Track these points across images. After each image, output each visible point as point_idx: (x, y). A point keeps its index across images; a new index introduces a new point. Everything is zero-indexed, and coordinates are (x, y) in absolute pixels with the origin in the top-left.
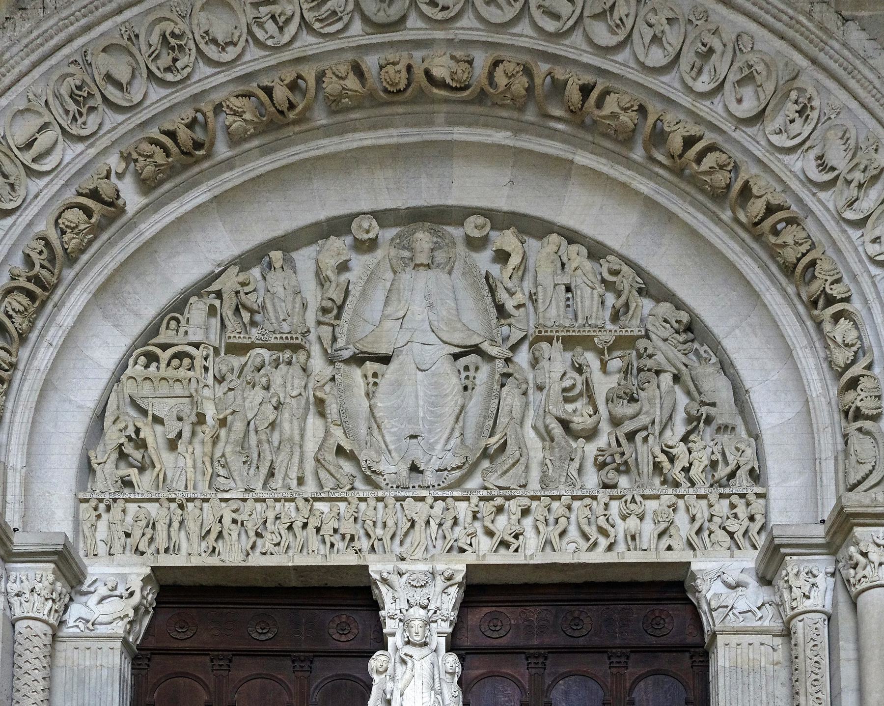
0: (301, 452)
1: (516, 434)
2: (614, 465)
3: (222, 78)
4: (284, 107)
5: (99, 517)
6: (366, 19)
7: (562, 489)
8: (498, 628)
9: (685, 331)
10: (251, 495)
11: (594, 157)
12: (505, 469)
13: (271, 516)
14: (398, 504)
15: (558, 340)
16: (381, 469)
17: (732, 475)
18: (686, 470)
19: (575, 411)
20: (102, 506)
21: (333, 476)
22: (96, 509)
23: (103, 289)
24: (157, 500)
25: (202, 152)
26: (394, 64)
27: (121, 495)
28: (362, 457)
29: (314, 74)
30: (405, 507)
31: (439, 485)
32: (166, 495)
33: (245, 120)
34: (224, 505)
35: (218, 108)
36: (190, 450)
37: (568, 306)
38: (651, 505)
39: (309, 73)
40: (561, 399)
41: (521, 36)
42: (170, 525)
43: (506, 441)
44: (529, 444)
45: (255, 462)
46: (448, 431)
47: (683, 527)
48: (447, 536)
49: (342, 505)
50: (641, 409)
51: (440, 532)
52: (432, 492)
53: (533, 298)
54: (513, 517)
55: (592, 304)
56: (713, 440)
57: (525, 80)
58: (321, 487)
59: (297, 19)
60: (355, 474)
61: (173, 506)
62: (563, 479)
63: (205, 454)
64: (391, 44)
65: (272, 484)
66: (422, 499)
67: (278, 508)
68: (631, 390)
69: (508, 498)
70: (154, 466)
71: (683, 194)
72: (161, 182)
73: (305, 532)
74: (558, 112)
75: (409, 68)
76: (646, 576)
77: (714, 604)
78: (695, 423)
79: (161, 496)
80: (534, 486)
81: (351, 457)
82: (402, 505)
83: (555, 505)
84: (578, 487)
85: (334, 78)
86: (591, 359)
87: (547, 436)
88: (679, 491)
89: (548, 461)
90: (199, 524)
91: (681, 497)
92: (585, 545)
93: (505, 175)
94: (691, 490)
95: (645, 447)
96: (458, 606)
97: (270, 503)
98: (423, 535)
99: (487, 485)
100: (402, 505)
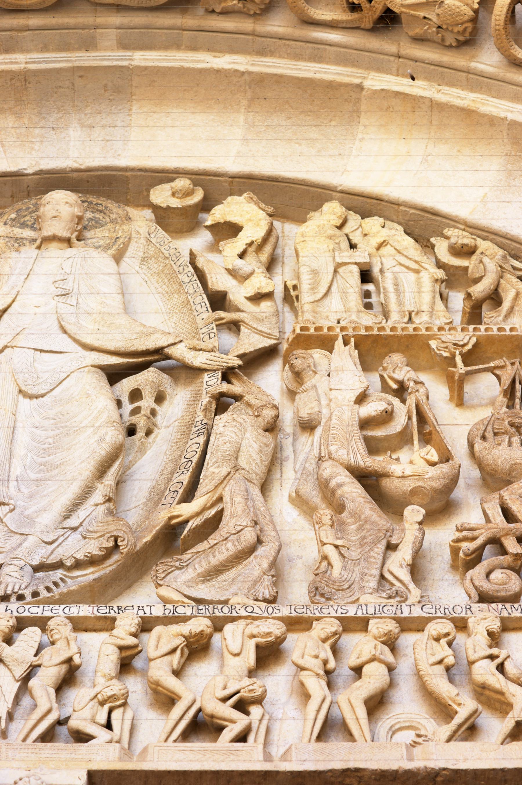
2: (507, 559)
31: (35, 594)
62: (372, 583)
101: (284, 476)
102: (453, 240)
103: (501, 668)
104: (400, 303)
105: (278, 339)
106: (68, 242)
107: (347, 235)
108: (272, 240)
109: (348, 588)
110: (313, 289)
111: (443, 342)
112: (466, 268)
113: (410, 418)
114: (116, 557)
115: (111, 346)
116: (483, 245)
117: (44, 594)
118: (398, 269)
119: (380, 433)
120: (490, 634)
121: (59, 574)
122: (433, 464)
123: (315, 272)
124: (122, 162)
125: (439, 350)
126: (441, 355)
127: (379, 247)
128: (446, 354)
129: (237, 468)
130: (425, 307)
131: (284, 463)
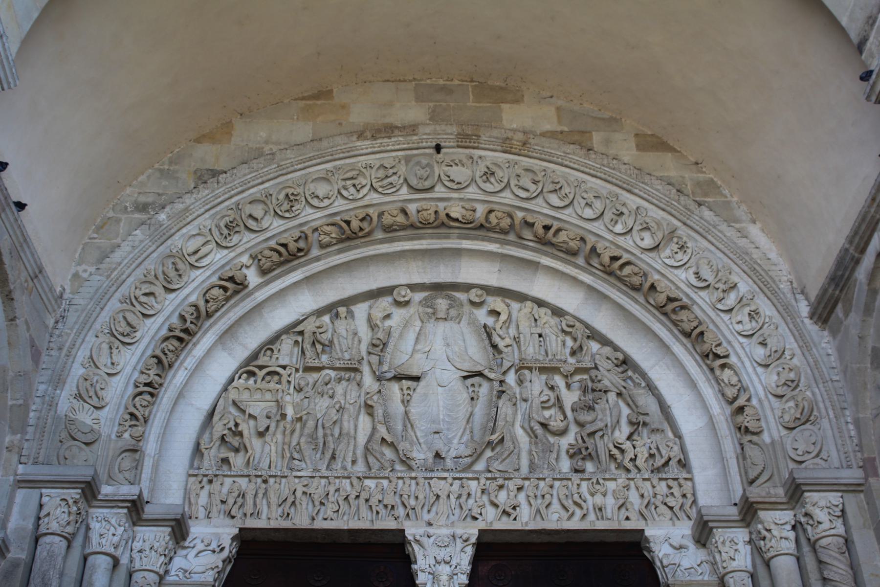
0: (355, 443)
1: (510, 433)
2: (581, 456)
3: (319, 214)
4: (357, 230)
5: (202, 488)
6: (410, 186)
7: (546, 473)
8: (502, 578)
9: (621, 365)
10: (317, 474)
11: (554, 261)
12: (503, 457)
13: (332, 489)
14: (427, 481)
15: (536, 369)
16: (414, 456)
17: (666, 464)
18: (633, 460)
19: (550, 417)
20: (205, 479)
21: (379, 461)
22: (200, 482)
23: (226, 332)
24: (248, 476)
25: (302, 254)
26: (426, 210)
27: (220, 472)
28: (400, 447)
29: (376, 214)
30: (432, 485)
32: (255, 473)
33: (331, 238)
34: (297, 480)
35: (316, 230)
36: (275, 440)
37: (541, 346)
38: (611, 485)
39: (373, 213)
40: (540, 409)
41: (505, 198)
42: (256, 495)
43: (503, 438)
44: (519, 438)
45: (321, 449)
46: (462, 430)
47: (633, 497)
48: (464, 507)
49: (385, 482)
50: (597, 417)
51: (458, 503)
52: (451, 474)
53: (517, 340)
54: (511, 493)
55: (557, 346)
56: (649, 438)
57: (509, 221)
58: (370, 468)
59: (369, 184)
60: (394, 459)
61: (259, 480)
62: (546, 466)
63: (284, 444)
64: (425, 199)
65: (334, 466)
66: (445, 478)
67: (337, 484)
68: (589, 404)
69: (505, 479)
70: (247, 451)
71: (613, 286)
72: (274, 269)
73: (357, 502)
74: (531, 238)
75: (436, 212)
76: (612, 538)
77: (665, 562)
78: (636, 427)
79: (251, 473)
80: (525, 470)
81: (392, 445)
82: (429, 483)
83: (542, 484)
84: (557, 472)
85: (390, 217)
86: (559, 381)
87: (532, 434)
88: (630, 476)
89: (534, 453)
90: (277, 495)
91: (633, 479)
92: (565, 515)
93: (496, 267)
94: (638, 475)
95: (602, 442)
96: (471, 561)
97: (332, 480)
98: (446, 507)
99: (491, 469)
100: (429, 483)
103: (580, 496)
104: (551, 350)
106: (445, 319)
110: (525, 344)
114: (475, 454)
115: (465, 369)
116: (578, 324)
117: (459, 469)
118: (550, 334)
120: (578, 485)
121: (461, 459)
122: (562, 421)
123: (525, 337)
124: (459, 281)
127: (545, 324)
129: (507, 422)
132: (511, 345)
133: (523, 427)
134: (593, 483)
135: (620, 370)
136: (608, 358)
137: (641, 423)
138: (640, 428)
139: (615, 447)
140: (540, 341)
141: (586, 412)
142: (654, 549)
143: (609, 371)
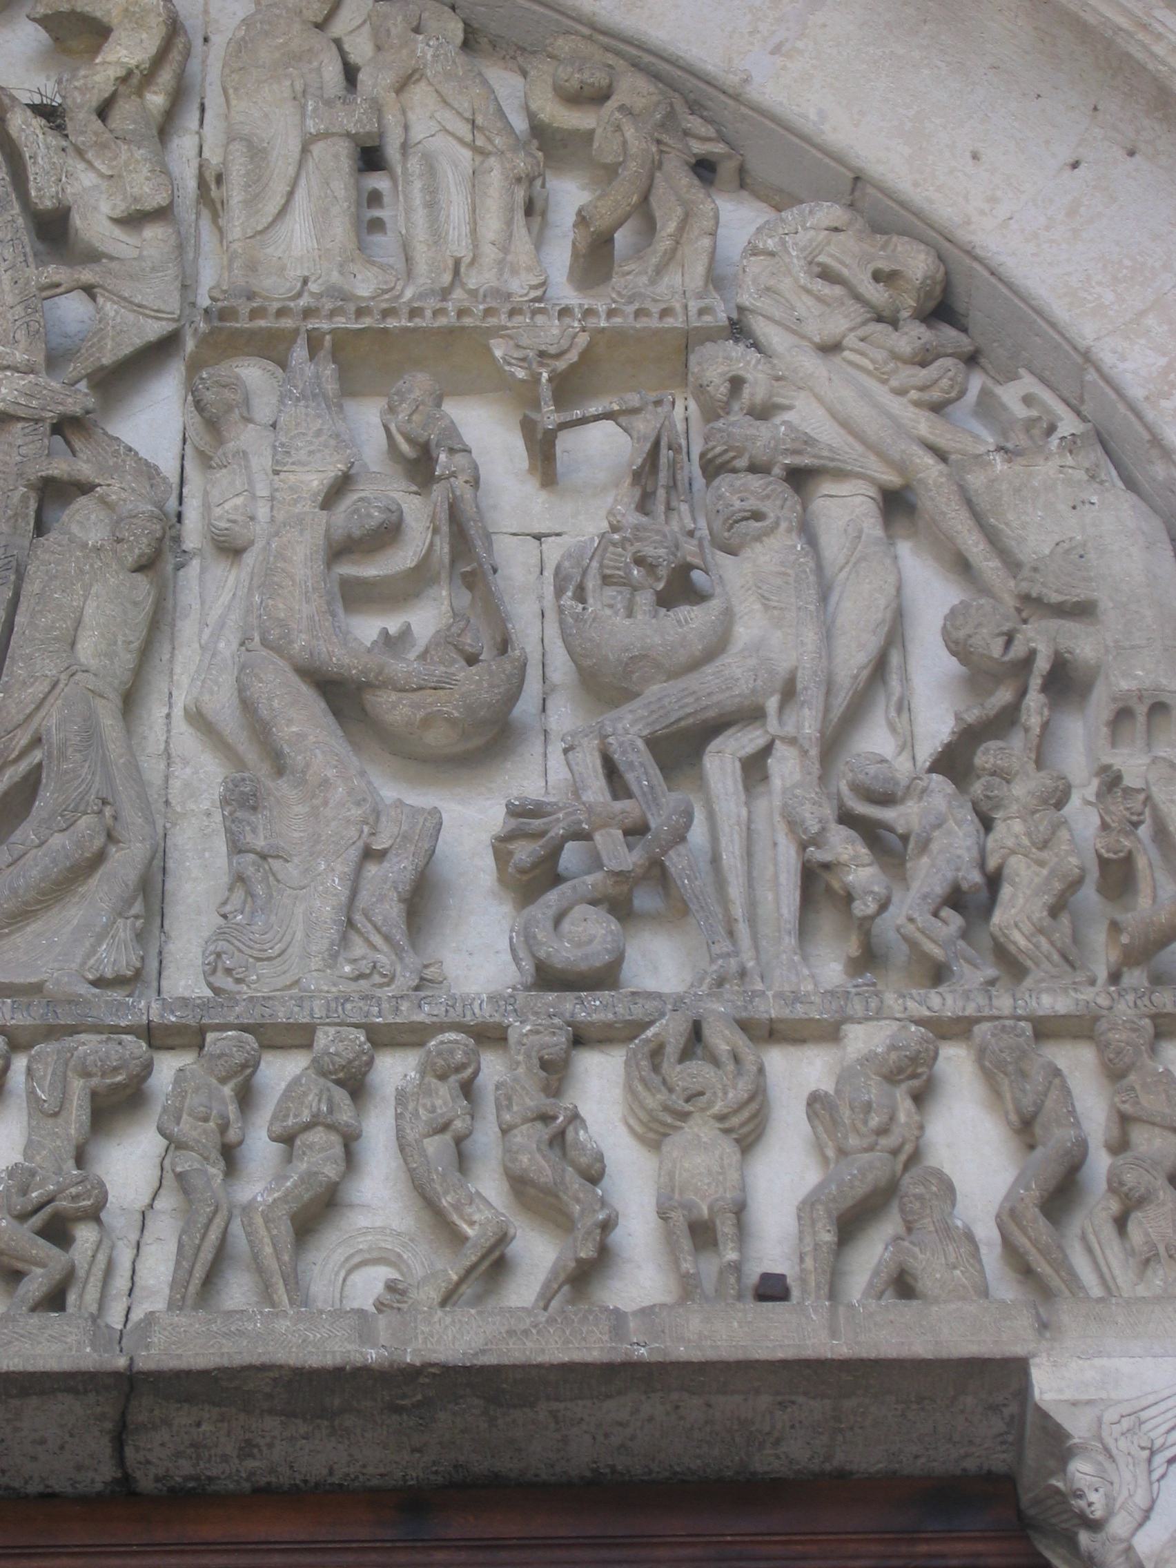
101: (180, 658)
102: (563, 72)
104: (437, 236)
105: (178, 320)
107: (338, 43)
108: (175, 56)
109: (279, 955)
111: (518, 346)
112: (589, 135)
113: (436, 531)
118: (441, 143)
119: (370, 570)
125: (510, 364)
126: (512, 374)
128: (521, 374)
130: (490, 253)
131: (179, 624)
132: (162, 214)
133: (199, 719)
134: (656, 1053)
135: (913, 336)
136: (826, 275)
137: (1042, 664)
138: (1034, 699)
139: (847, 818)
140: (375, 198)
141: (645, 600)
142: (1096, 1502)
143: (830, 348)
